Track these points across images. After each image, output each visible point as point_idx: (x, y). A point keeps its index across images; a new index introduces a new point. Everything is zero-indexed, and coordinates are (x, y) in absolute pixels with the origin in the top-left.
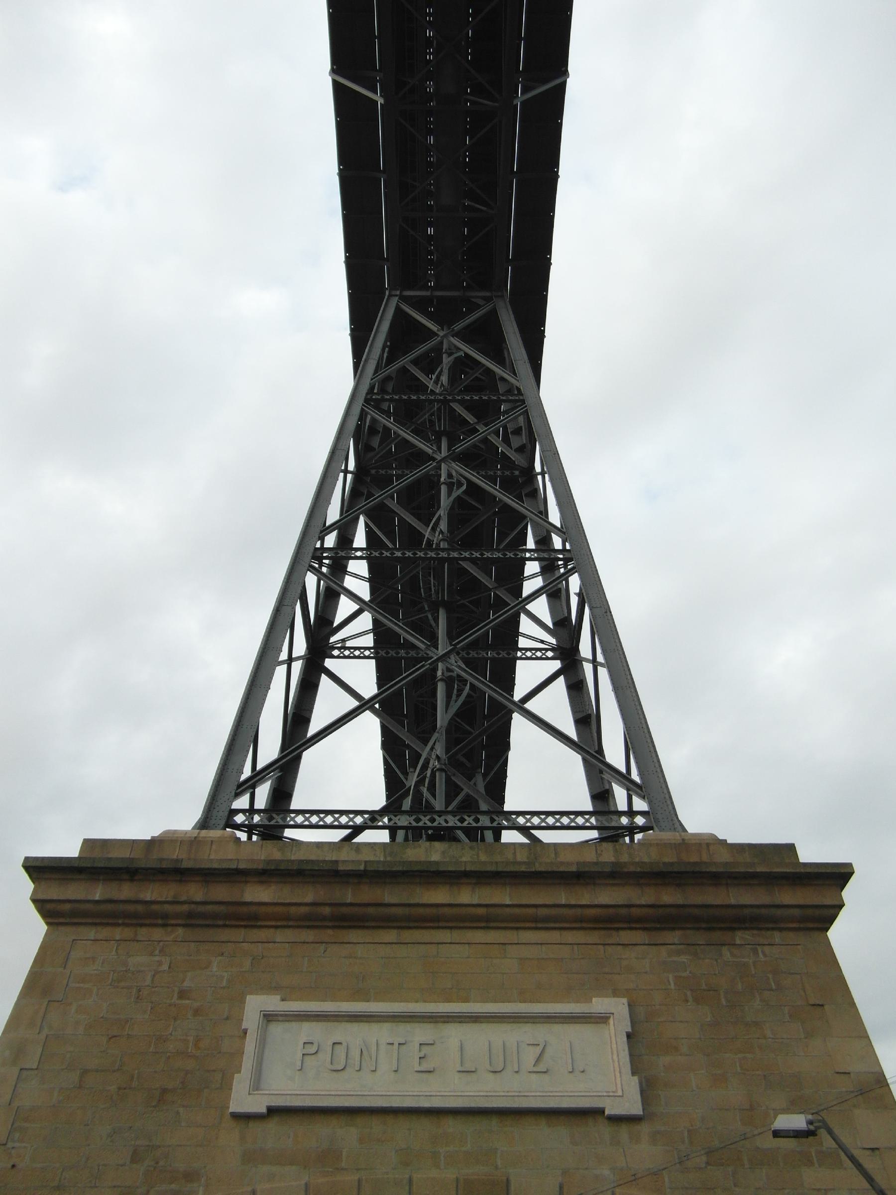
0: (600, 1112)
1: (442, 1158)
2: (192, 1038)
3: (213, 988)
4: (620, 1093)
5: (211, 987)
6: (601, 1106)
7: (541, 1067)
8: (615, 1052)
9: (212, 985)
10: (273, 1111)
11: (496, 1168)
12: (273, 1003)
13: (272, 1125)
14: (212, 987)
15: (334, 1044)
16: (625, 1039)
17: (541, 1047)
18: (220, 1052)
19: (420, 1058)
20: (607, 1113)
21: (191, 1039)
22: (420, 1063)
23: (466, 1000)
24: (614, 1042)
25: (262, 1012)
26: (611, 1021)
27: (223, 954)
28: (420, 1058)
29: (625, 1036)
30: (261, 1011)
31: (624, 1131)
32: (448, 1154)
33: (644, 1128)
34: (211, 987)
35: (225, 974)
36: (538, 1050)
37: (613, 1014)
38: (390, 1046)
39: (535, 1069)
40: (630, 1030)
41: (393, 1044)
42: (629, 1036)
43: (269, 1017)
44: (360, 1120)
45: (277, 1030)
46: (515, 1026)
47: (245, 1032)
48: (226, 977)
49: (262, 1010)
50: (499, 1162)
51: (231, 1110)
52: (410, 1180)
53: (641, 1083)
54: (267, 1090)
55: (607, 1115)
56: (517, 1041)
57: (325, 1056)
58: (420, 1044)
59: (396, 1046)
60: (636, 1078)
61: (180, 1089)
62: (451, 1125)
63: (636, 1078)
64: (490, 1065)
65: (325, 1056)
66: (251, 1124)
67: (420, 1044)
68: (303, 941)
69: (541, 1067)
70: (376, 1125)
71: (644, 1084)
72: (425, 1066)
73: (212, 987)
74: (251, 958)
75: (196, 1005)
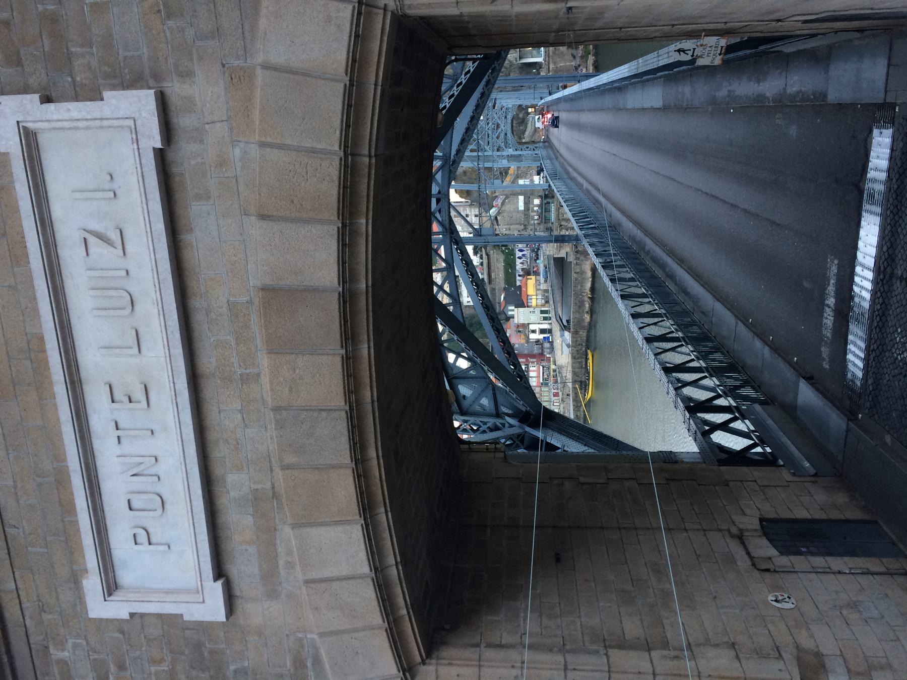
0: (162, 158)
1: (248, 371)
2: (152, 668)
3: (91, 653)
4: (131, 123)
5: (89, 655)
6: (151, 155)
7: (114, 236)
8: (75, 124)
9: (86, 654)
10: (220, 572)
11: (250, 302)
12: (92, 584)
13: (234, 570)
14: (88, 654)
15: (131, 509)
16: (52, 106)
17: (88, 236)
18: (163, 636)
19: (130, 402)
20: (159, 145)
21: (153, 669)
22: (139, 402)
23: (41, 339)
24: (59, 124)
25: (106, 599)
26: (30, 125)
27: (46, 647)
28: (130, 402)
29: (48, 105)
30: (105, 600)
31: (183, 121)
32: (242, 364)
33: (176, 89)
34: (89, 655)
35: (70, 642)
36: (92, 240)
37: (18, 122)
38: (122, 440)
39: (120, 247)
40: (36, 97)
41: (119, 437)
42: (47, 99)
43: (111, 587)
44: (217, 470)
45: (125, 577)
46: (65, 273)
47: (132, 615)
48: (74, 641)
49: (103, 599)
50: (245, 299)
51: (224, 620)
52: (276, 409)
53: (113, 87)
54: (197, 584)
55: (162, 145)
56: (86, 270)
57: (147, 520)
58: (113, 402)
59: (119, 433)
60: (107, 94)
61: (209, 672)
62: (208, 362)
63: (107, 94)
64: (124, 308)
65: (147, 520)
66: (237, 592)
67: (113, 402)
68: (7, 557)
69: (114, 236)
70: (220, 453)
71: (114, 81)
72: (139, 395)
73: (88, 654)
74: (43, 613)
75: (113, 668)
